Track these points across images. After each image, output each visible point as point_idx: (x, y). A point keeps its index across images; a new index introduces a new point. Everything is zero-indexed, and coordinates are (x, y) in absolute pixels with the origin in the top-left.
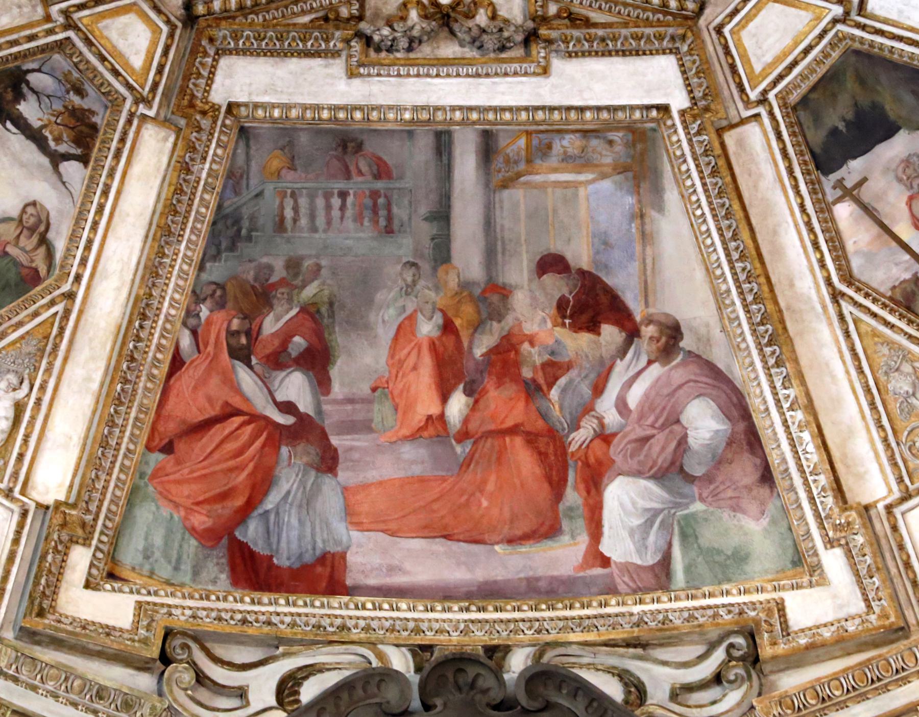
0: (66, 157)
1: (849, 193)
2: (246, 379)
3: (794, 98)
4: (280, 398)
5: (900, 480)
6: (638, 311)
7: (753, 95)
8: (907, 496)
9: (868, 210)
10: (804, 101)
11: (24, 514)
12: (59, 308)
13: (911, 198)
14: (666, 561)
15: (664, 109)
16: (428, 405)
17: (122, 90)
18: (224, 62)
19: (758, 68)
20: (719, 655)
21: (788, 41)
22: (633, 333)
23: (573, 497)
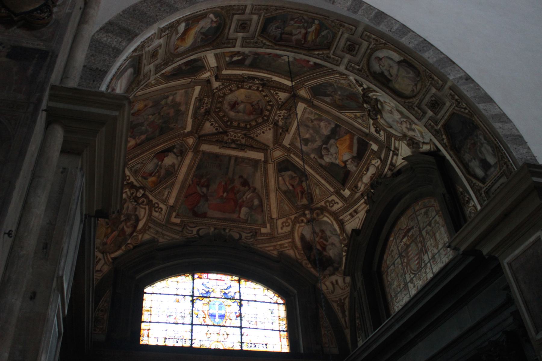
0: (179, 156)
1: (282, 176)
2: (198, 188)
3: (278, 162)
4: (202, 191)
5: (279, 217)
6: (251, 186)
7: (273, 161)
8: (279, 219)
9: (284, 179)
10: (279, 163)
11: (168, 208)
12: (175, 178)
13: (289, 180)
14: (248, 219)
15: (261, 160)
16: (221, 194)
17: (188, 147)
18: (202, 145)
19: (274, 157)
20: (251, 234)
21: (279, 155)
22: (250, 188)
23: (238, 209)
